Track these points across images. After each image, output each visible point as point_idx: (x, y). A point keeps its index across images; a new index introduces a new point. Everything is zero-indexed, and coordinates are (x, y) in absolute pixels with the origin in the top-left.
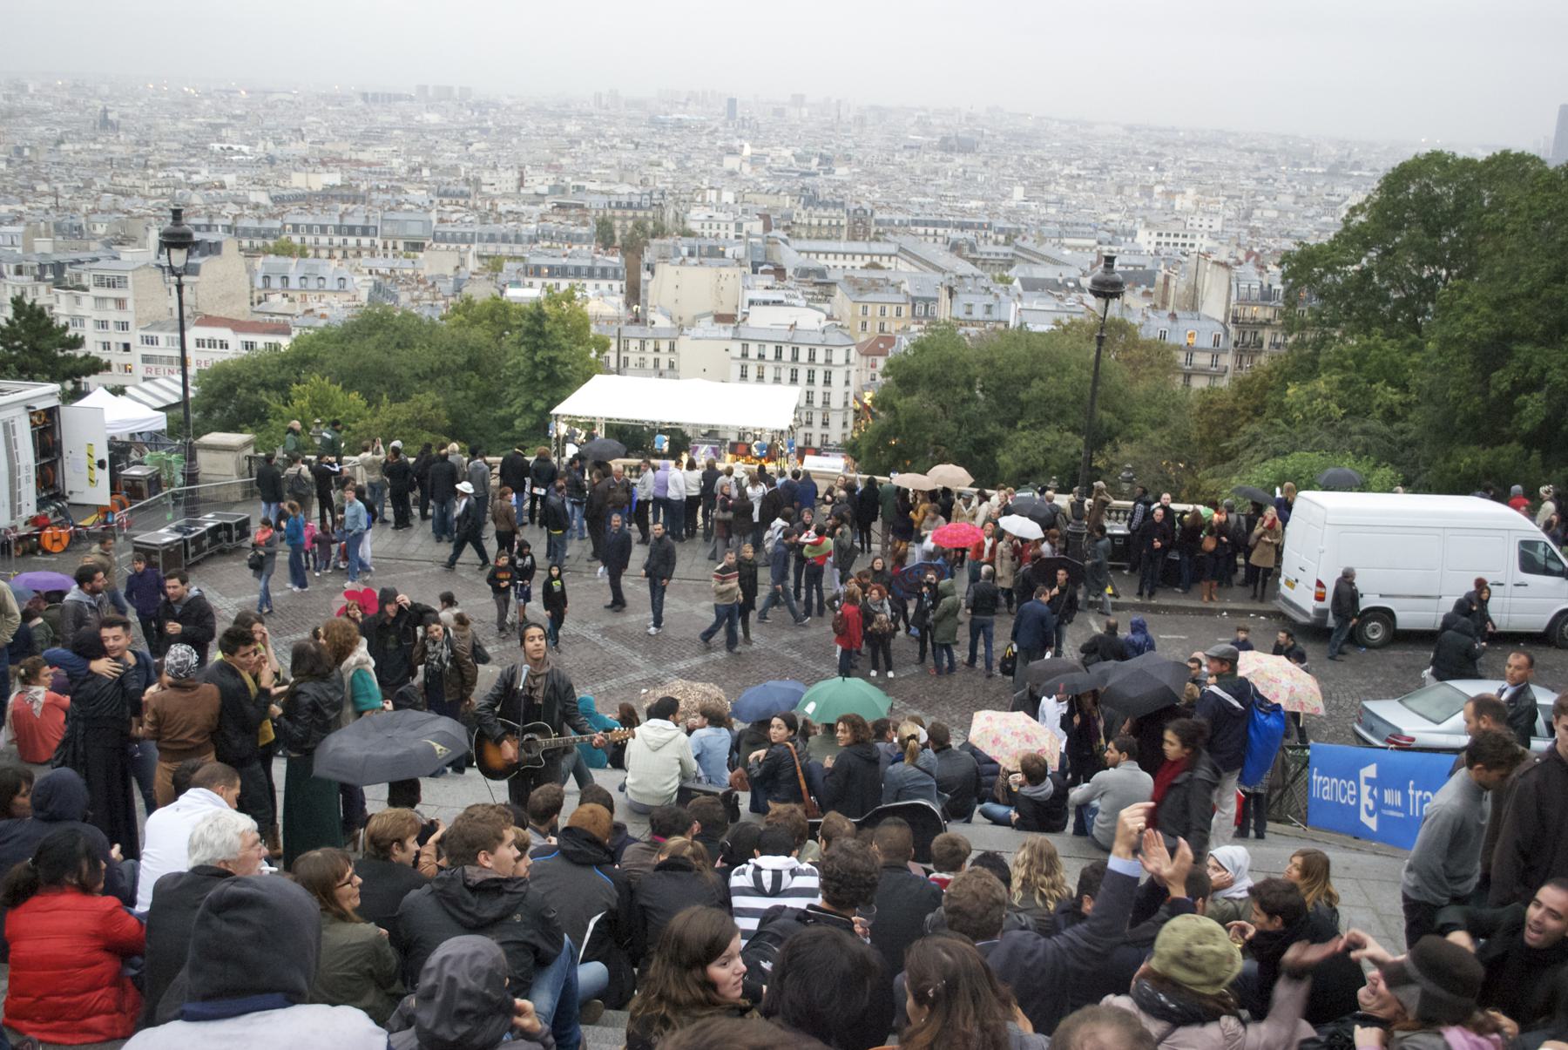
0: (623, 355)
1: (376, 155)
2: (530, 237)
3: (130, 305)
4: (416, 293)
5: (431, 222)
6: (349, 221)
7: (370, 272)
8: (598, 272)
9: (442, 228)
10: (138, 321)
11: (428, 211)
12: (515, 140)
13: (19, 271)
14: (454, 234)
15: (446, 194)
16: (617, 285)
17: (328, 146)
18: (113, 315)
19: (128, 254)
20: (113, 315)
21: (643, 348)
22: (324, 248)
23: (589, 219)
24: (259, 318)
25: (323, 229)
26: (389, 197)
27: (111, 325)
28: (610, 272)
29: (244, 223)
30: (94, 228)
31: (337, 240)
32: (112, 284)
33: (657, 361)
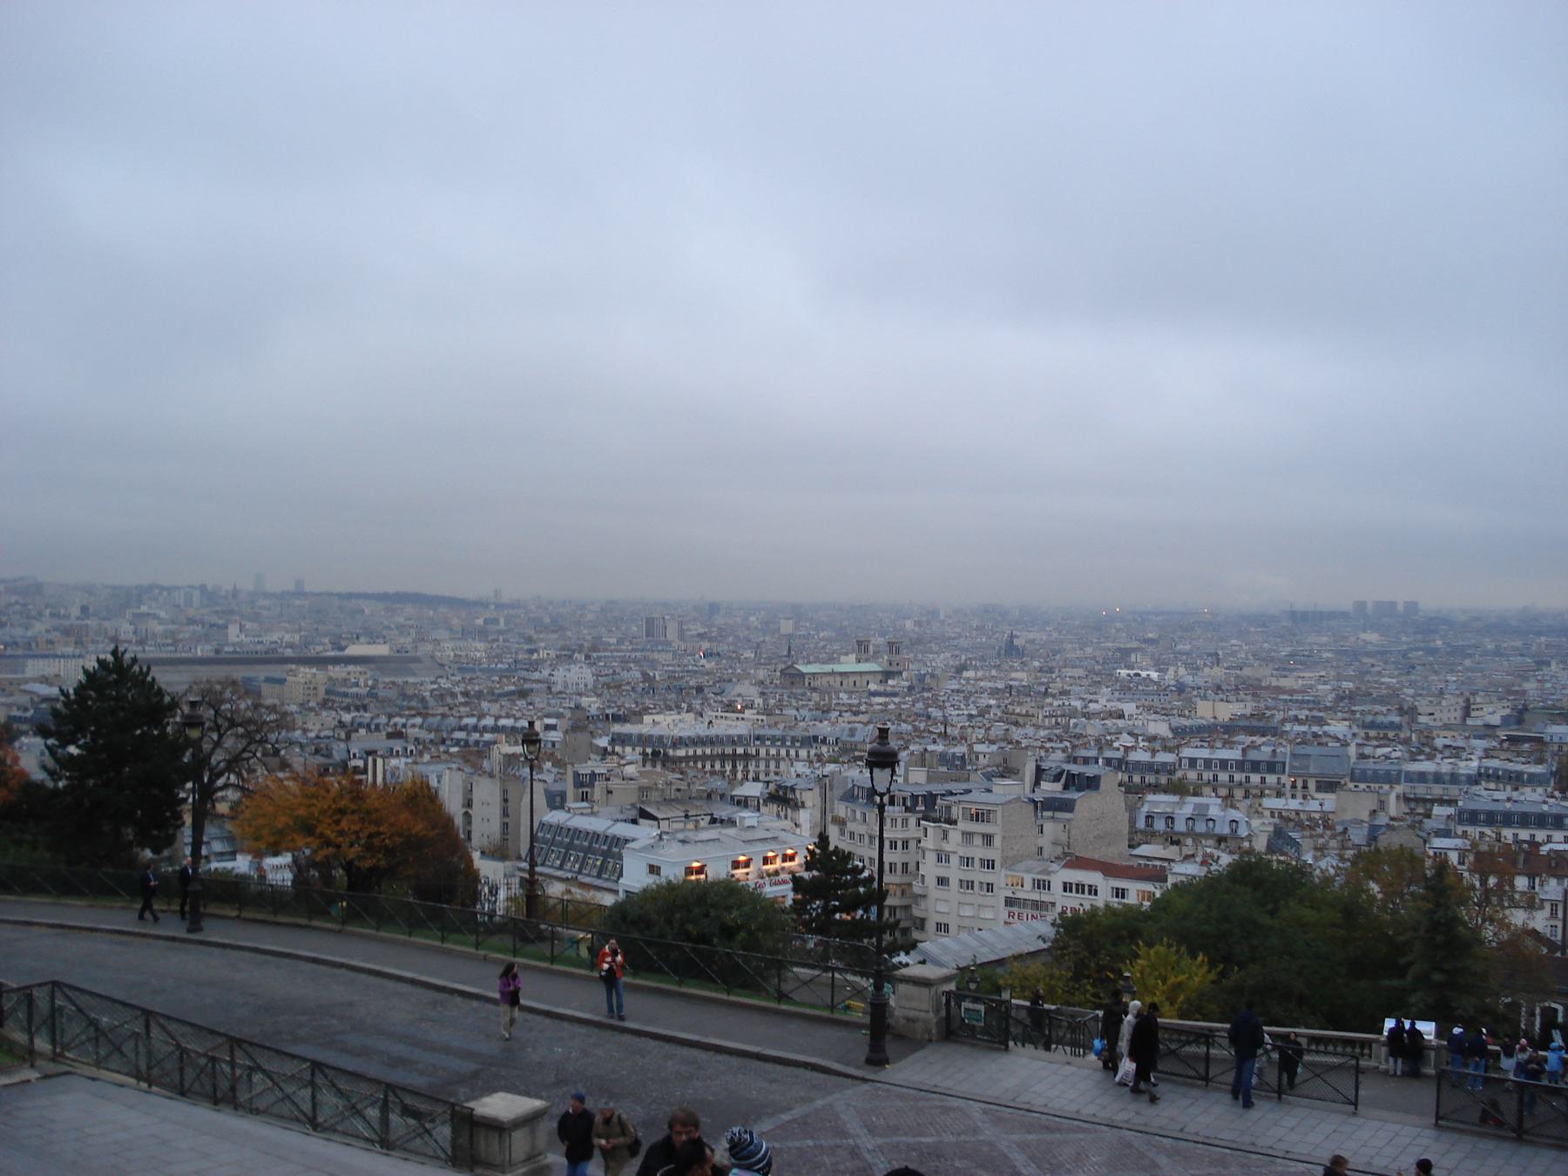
1: (1300, 681)
2: (1469, 777)
3: (997, 841)
4: (1321, 841)
6: (1253, 755)
10: (1005, 860)
11: (1345, 745)
12: (1468, 663)
14: (1375, 771)
15: (1372, 725)
17: (1247, 672)
18: (978, 852)
19: (1005, 789)
20: (978, 852)
24: (1134, 862)
25: (1224, 764)
26: (1304, 728)
27: (977, 863)
29: (1135, 756)
30: (977, 758)
31: (1238, 777)
32: (978, 817)
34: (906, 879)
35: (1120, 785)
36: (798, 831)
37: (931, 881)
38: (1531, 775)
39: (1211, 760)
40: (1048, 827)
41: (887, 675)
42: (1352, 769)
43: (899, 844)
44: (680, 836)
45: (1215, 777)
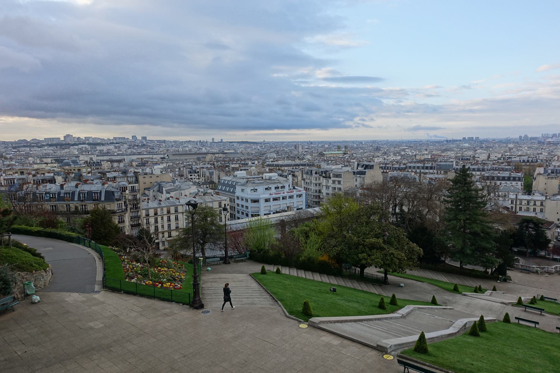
0: (518, 207)
2: (487, 169)
3: (342, 183)
5: (453, 165)
6: (426, 165)
7: (430, 178)
8: (512, 178)
9: (457, 167)
12: (491, 149)
13: (316, 173)
16: (519, 183)
17: (433, 153)
21: (528, 204)
22: (418, 173)
23: (511, 164)
25: (418, 168)
28: (517, 179)
31: (422, 171)
33: (534, 210)
34: (319, 194)
35: (380, 168)
36: (288, 181)
37: (325, 194)
38: (507, 169)
39: (415, 167)
40: (358, 179)
41: (345, 154)
42: (454, 168)
43: (318, 185)
44: (253, 182)
45: (416, 171)
